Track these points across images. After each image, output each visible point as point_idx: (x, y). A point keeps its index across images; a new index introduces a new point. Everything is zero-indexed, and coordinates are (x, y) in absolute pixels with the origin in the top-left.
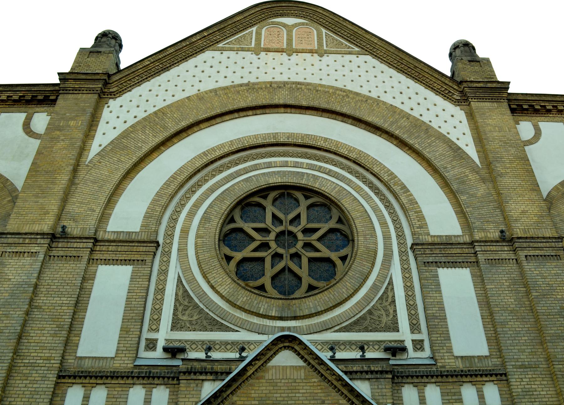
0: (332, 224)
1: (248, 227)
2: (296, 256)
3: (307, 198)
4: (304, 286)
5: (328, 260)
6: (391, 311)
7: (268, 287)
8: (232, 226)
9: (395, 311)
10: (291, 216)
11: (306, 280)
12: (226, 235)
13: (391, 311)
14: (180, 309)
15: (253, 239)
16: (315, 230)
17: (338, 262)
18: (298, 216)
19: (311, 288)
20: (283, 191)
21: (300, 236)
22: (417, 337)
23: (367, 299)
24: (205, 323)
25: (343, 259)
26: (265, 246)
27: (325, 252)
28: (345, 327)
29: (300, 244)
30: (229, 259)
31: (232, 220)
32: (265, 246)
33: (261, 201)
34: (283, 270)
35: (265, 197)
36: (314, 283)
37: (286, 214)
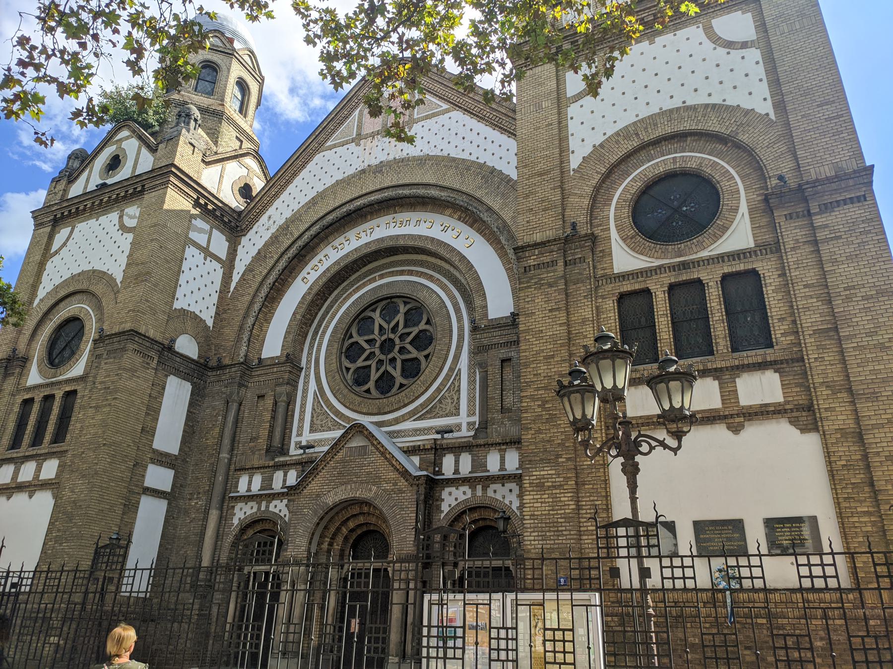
0: (422, 326)
1: (361, 341)
3: (406, 303)
4: (397, 385)
5: (416, 358)
6: (455, 399)
7: (373, 390)
9: (458, 399)
11: (399, 380)
12: (348, 349)
13: (455, 399)
14: (315, 416)
15: (366, 350)
16: (409, 334)
17: (423, 360)
18: (397, 324)
19: (402, 386)
20: (389, 300)
21: (397, 341)
22: (472, 419)
23: (439, 390)
24: (330, 424)
25: (427, 357)
27: (414, 354)
28: (420, 416)
29: (397, 348)
31: (351, 336)
32: (372, 354)
33: (372, 314)
34: (384, 373)
35: (374, 310)
36: (404, 382)
37: (389, 323)
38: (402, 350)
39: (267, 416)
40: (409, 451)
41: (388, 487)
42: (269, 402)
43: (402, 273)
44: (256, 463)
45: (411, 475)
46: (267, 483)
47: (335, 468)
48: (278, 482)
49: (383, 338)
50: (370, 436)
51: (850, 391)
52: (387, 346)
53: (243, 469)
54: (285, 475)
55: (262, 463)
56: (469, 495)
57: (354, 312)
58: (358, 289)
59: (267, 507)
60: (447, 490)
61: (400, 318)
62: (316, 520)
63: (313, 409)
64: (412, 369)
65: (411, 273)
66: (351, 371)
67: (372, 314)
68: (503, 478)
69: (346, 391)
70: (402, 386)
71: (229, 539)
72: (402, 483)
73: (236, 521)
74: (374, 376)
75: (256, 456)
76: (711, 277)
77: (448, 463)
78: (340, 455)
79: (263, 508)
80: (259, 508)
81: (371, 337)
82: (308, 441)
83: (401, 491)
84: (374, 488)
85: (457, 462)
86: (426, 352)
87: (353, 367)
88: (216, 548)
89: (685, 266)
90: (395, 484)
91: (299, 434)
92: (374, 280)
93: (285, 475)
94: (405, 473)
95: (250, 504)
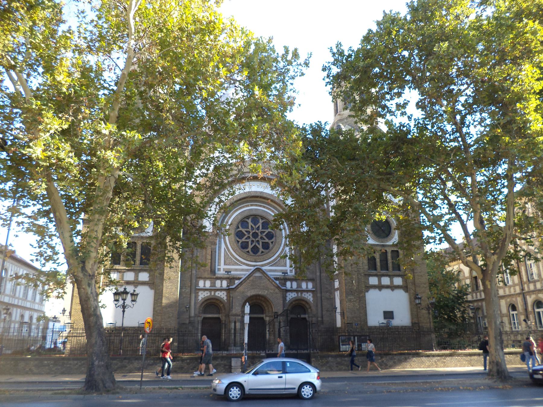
2: (258, 241)
3: (262, 219)
5: (267, 243)
8: (239, 230)
10: (257, 226)
11: (261, 250)
16: (264, 232)
17: (271, 244)
19: (262, 252)
21: (259, 234)
25: (272, 242)
26: (249, 237)
27: (267, 240)
29: (259, 237)
30: (238, 242)
31: (238, 228)
32: (249, 237)
33: (247, 220)
35: (248, 219)
36: (263, 251)
38: (262, 238)
39: (209, 257)
40: (277, 279)
41: (272, 291)
42: (209, 252)
43: (260, 206)
44: (207, 276)
45: (280, 288)
46: (213, 285)
47: (249, 283)
48: (218, 283)
49: (254, 231)
50: (263, 272)
51: (415, 284)
52: (255, 235)
53: (201, 278)
54: (221, 282)
55: (210, 276)
56: (296, 295)
57: (240, 218)
58: (241, 208)
59: (215, 294)
60: (288, 293)
61: (260, 224)
62: (244, 301)
63: (225, 256)
64: (266, 246)
65: (264, 207)
66: (240, 243)
67: (247, 220)
68: (307, 291)
69: (240, 251)
70: (262, 252)
71: (198, 305)
72: (277, 290)
73: (200, 298)
74: (250, 246)
75: (206, 273)
76: (389, 250)
77: (288, 284)
78: (251, 278)
79: (213, 294)
80: (211, 294)
81: (248, 230)
82: (224, 269)
83: (277, 293)
84: (266, 291)
85: (291, 284)
86: (272, 241)
87: (241, 241)
88: (195, 309)
89: (383, 246)
90: (274, 291)
91: (219, 265)
92: (248, 206)
93: (221, 282)
94: (278, 287)
95: (206, 292)
